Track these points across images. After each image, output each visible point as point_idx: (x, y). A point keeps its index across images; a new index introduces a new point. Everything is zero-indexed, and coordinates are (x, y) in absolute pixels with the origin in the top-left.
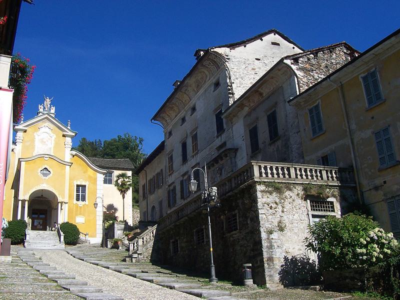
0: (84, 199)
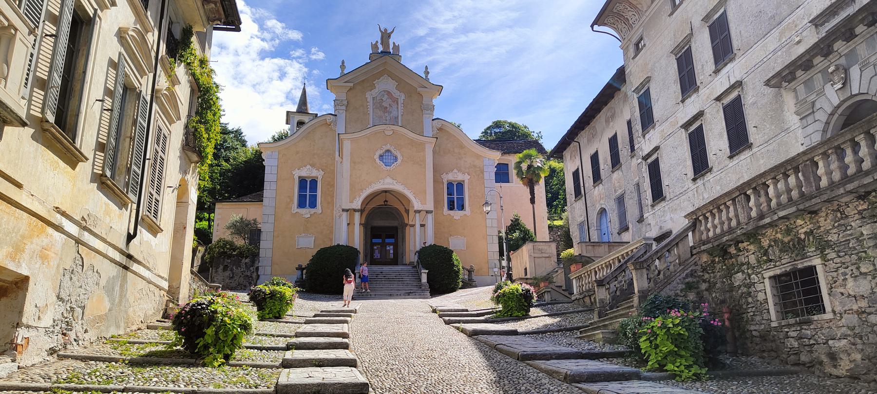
0: (462, 207)
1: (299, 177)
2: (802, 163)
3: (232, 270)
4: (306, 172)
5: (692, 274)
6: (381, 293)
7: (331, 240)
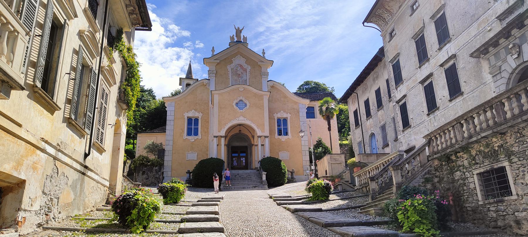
1: (188, 117)
2: (494, 104)
3: (147, 174)
4: (192, 114)
5: (429, 172)
6: (238, 187)
7: (207, 155)
